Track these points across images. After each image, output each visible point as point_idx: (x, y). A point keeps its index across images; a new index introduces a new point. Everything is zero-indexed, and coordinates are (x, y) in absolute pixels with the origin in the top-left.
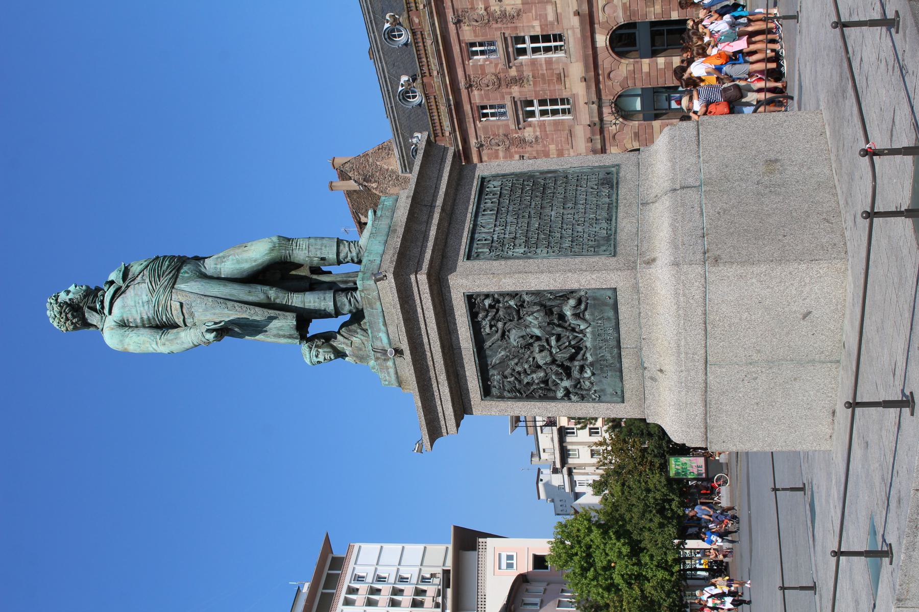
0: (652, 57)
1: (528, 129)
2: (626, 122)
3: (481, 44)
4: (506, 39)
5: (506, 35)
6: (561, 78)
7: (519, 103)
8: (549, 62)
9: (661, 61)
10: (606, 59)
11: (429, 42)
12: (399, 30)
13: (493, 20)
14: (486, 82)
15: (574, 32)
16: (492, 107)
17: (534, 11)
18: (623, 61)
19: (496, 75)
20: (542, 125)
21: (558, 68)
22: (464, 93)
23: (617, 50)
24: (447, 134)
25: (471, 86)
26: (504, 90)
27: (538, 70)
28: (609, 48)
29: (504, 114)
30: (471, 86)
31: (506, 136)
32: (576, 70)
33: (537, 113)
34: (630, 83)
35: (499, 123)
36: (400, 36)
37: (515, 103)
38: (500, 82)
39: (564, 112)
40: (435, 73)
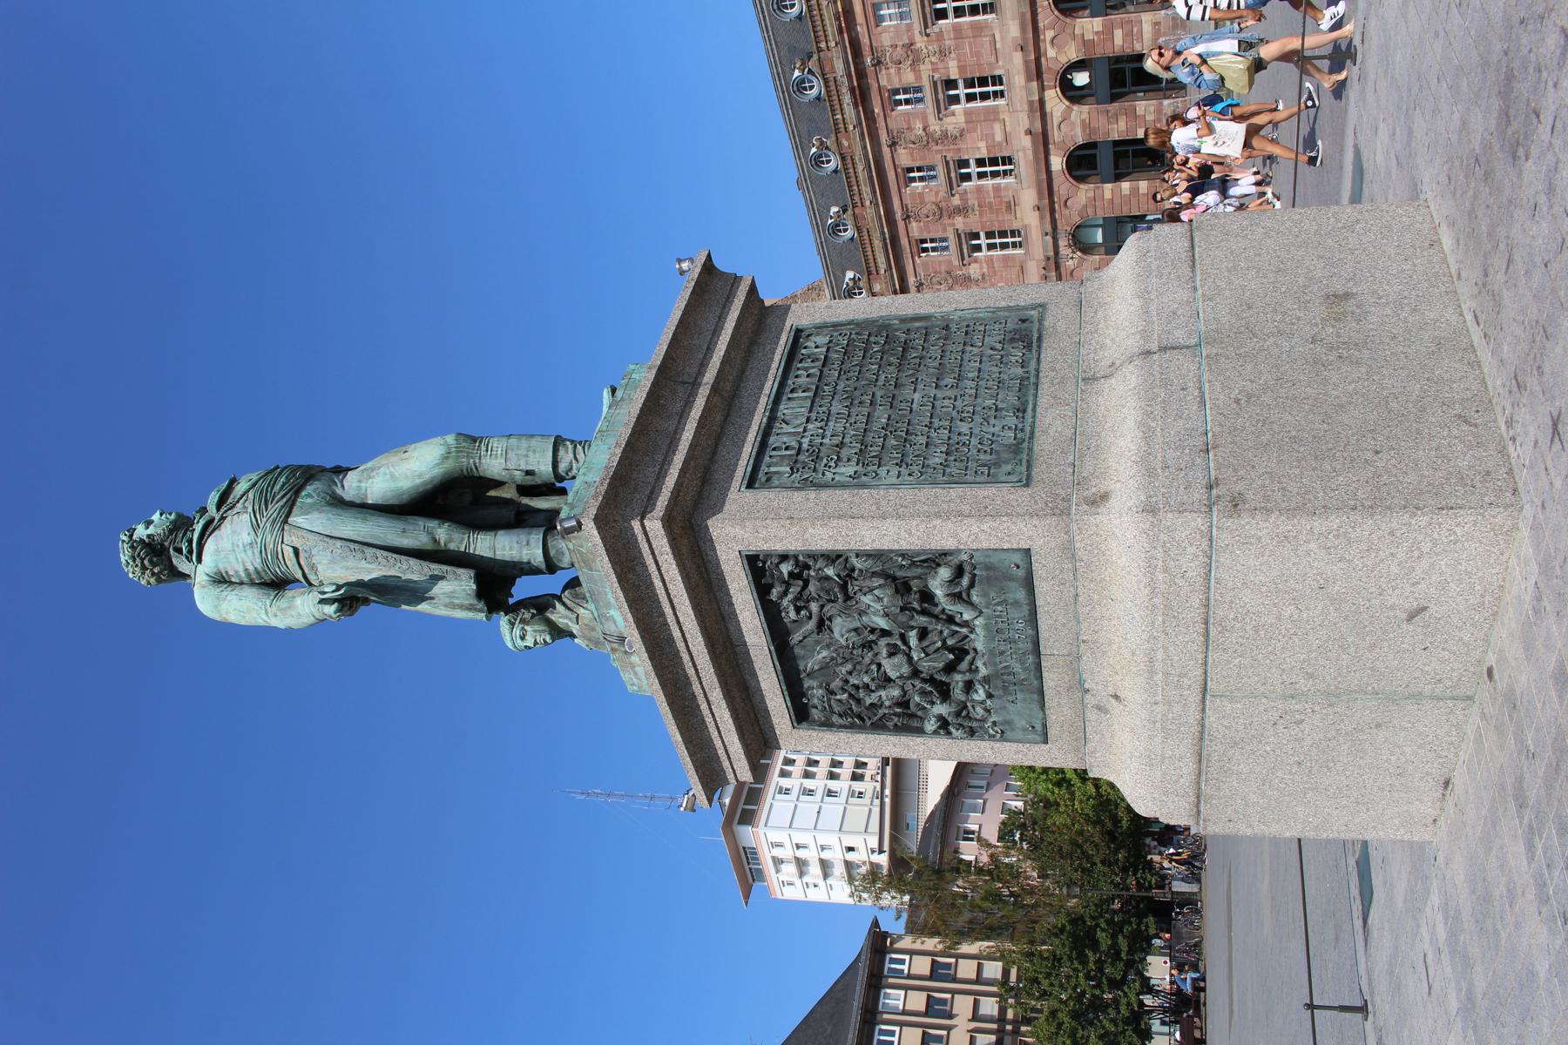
0: (1115, 182)
1: (973, 265)
2: (1085, 257)
3: (920, 169)
4: (947, 163)
5: (948, 159)
6: (1011, 206)
7: (963, 236)
8: (997, 188)
9: (1125, 186)
10: (1063, 184)
11: (860, 168)
12: (827, 156)
13: (933, 141)
14: (925, 212)
15: (1025, 155)
16: (932, 241)
17: (979, 131)
18: (1082, 186)
19: (937, 205)
20: (990, 260)
21: (1007, 196)
22: (901, 225)
23: (1074, 173)
24: (882, 272)
25: (908, 217)
26: (946, 221)
27: (984, 197)
28: (1066, 172)
29: (946, 248)
30: (908, 217)
31: (949, 273)
32: (1029, 198)
33: (984, 247)
34: (1090, 211)
35: (941, 259)
36: (828, 162)
37: (959, 235)
38: (941, 212)
39: (1014, 245)
40: (868, 203)
